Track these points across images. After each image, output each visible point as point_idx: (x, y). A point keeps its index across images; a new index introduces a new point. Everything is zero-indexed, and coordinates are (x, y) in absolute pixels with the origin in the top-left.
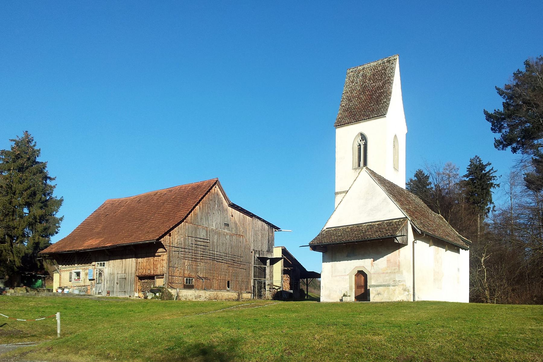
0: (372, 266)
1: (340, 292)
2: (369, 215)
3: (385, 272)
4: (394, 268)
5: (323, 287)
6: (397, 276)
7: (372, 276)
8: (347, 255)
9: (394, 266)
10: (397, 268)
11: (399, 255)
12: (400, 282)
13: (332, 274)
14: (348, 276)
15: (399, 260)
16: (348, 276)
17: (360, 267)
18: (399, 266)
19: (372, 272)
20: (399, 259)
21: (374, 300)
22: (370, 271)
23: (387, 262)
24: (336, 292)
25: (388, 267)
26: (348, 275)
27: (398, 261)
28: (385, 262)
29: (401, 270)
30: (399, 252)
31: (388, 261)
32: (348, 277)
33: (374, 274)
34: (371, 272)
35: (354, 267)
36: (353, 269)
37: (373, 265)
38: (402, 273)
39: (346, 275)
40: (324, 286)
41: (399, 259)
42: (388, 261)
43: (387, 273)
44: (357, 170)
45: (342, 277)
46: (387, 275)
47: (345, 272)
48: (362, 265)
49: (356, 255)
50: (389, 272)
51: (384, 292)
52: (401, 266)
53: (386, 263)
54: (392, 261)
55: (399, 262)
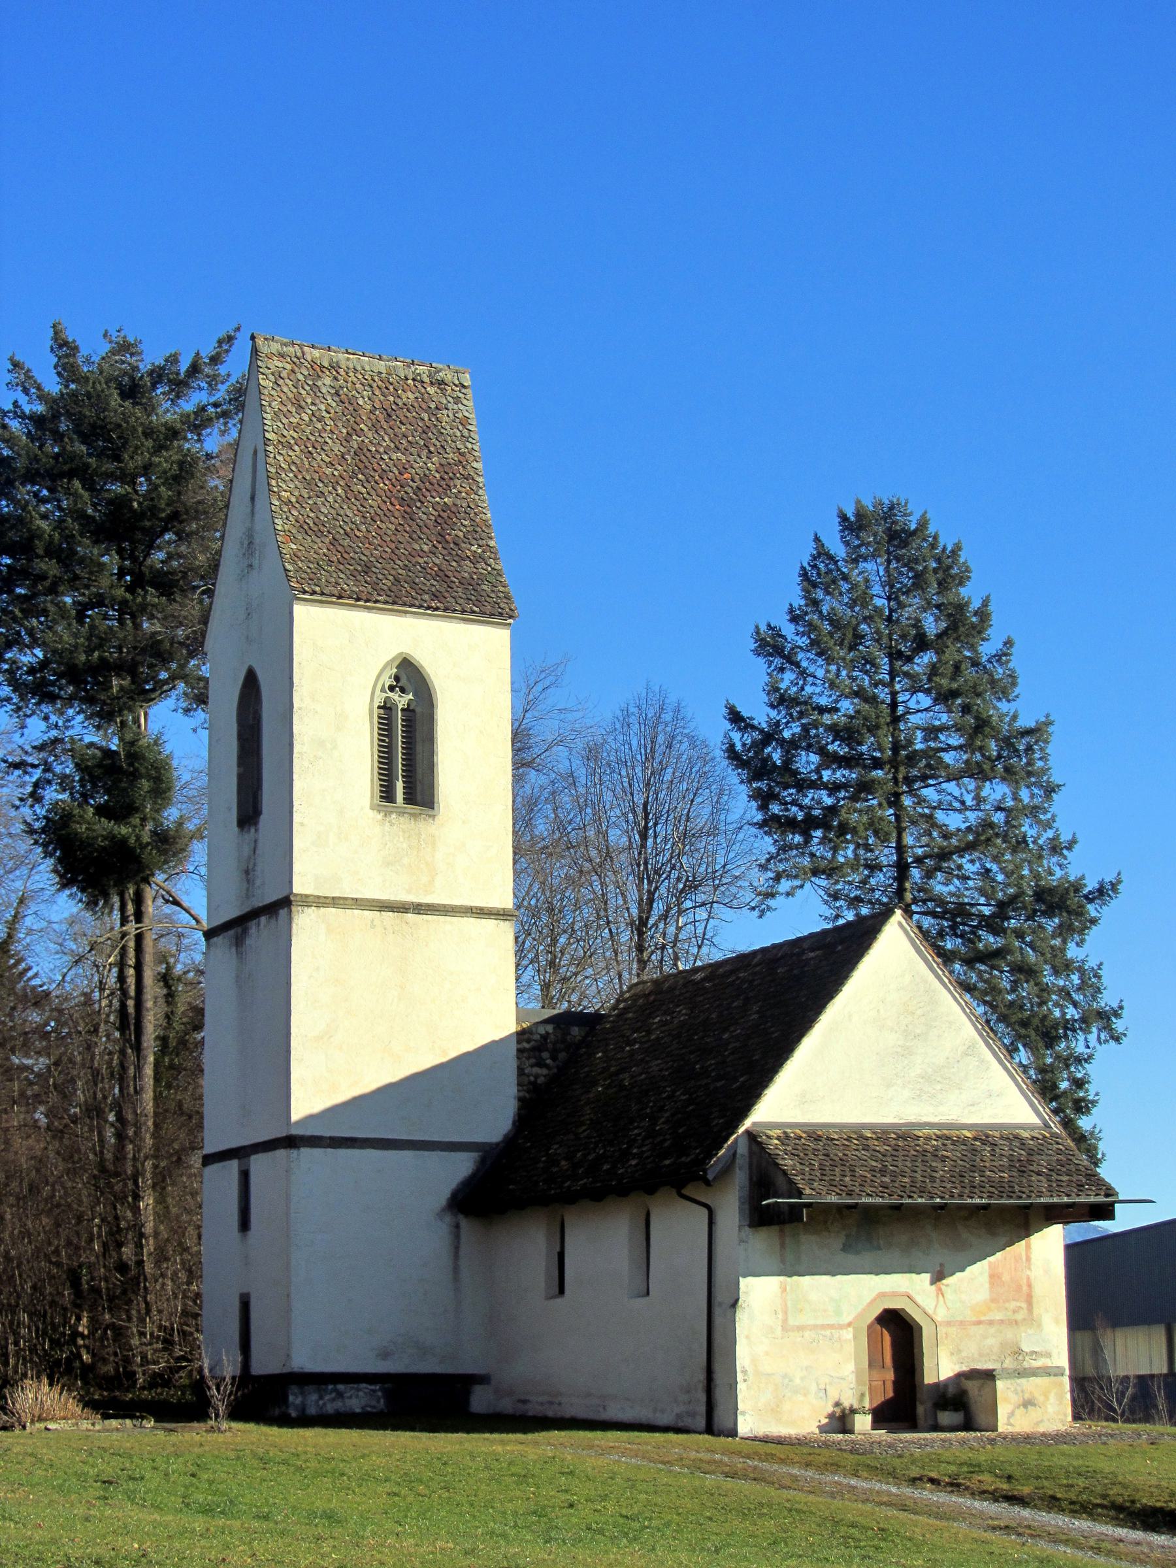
0: (940, 1296)
1: (822, 1394)
2: (919, 1096)
3: (983, 1318)
4: (1013, 1305)
5: (745, 1372)
6: (1023, 1334)
7: (942, 1331)
8: (844, 1245)
9: (1014, 1300)
10: (1024, 1305)
11: (1028, 1259)
12: (1034, 1357)
13: (785, 1321)
14: (851, 1329)
15: (1028, 1278)
16: (851, 1329)
17: (895, 1295)
18: (1029, 1299)
19: (940, 1315)
20: (1028, 1272)
21: (1011, 1425)
22: (930, 1312)
23: (990, 1283)
24: (805, 1395)
25: (993, 1300)
26: (849, 1325)
27: (1025, 1281)
28: (985, 1279)
29: (1036, 1311)
30: (1028, 1247)
31: (994, 1277)
32: (848, 1334)
33: (949, 1324)
34: (934, 1317)
35: (873, 1295)
36: (868, 1300)
37: (940, 1289)
38: (1040, 1325)
39: (841, 1327)
40: (750, 1370)
41: (1028, 1272)
42: (992, 1276)
43: (991, 1323)
44: (394, 816)
45: (828, 1333)
46: (992, 1330)
47: (838, 1312)
48: (902, 1290)
49: (879, 1248)
50: (998, 1318)
51: (1046, 1396)
52: (1034, 1300)
53: (987, 1285)
54: (1006, 1277)
55: (1029, 1286)
